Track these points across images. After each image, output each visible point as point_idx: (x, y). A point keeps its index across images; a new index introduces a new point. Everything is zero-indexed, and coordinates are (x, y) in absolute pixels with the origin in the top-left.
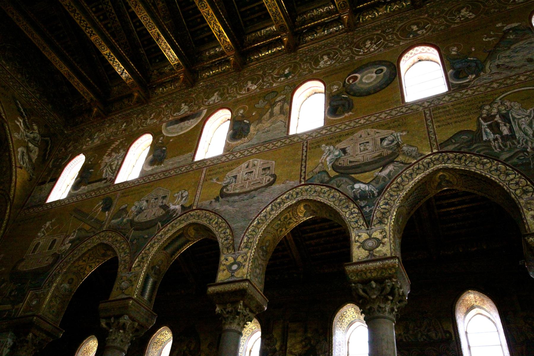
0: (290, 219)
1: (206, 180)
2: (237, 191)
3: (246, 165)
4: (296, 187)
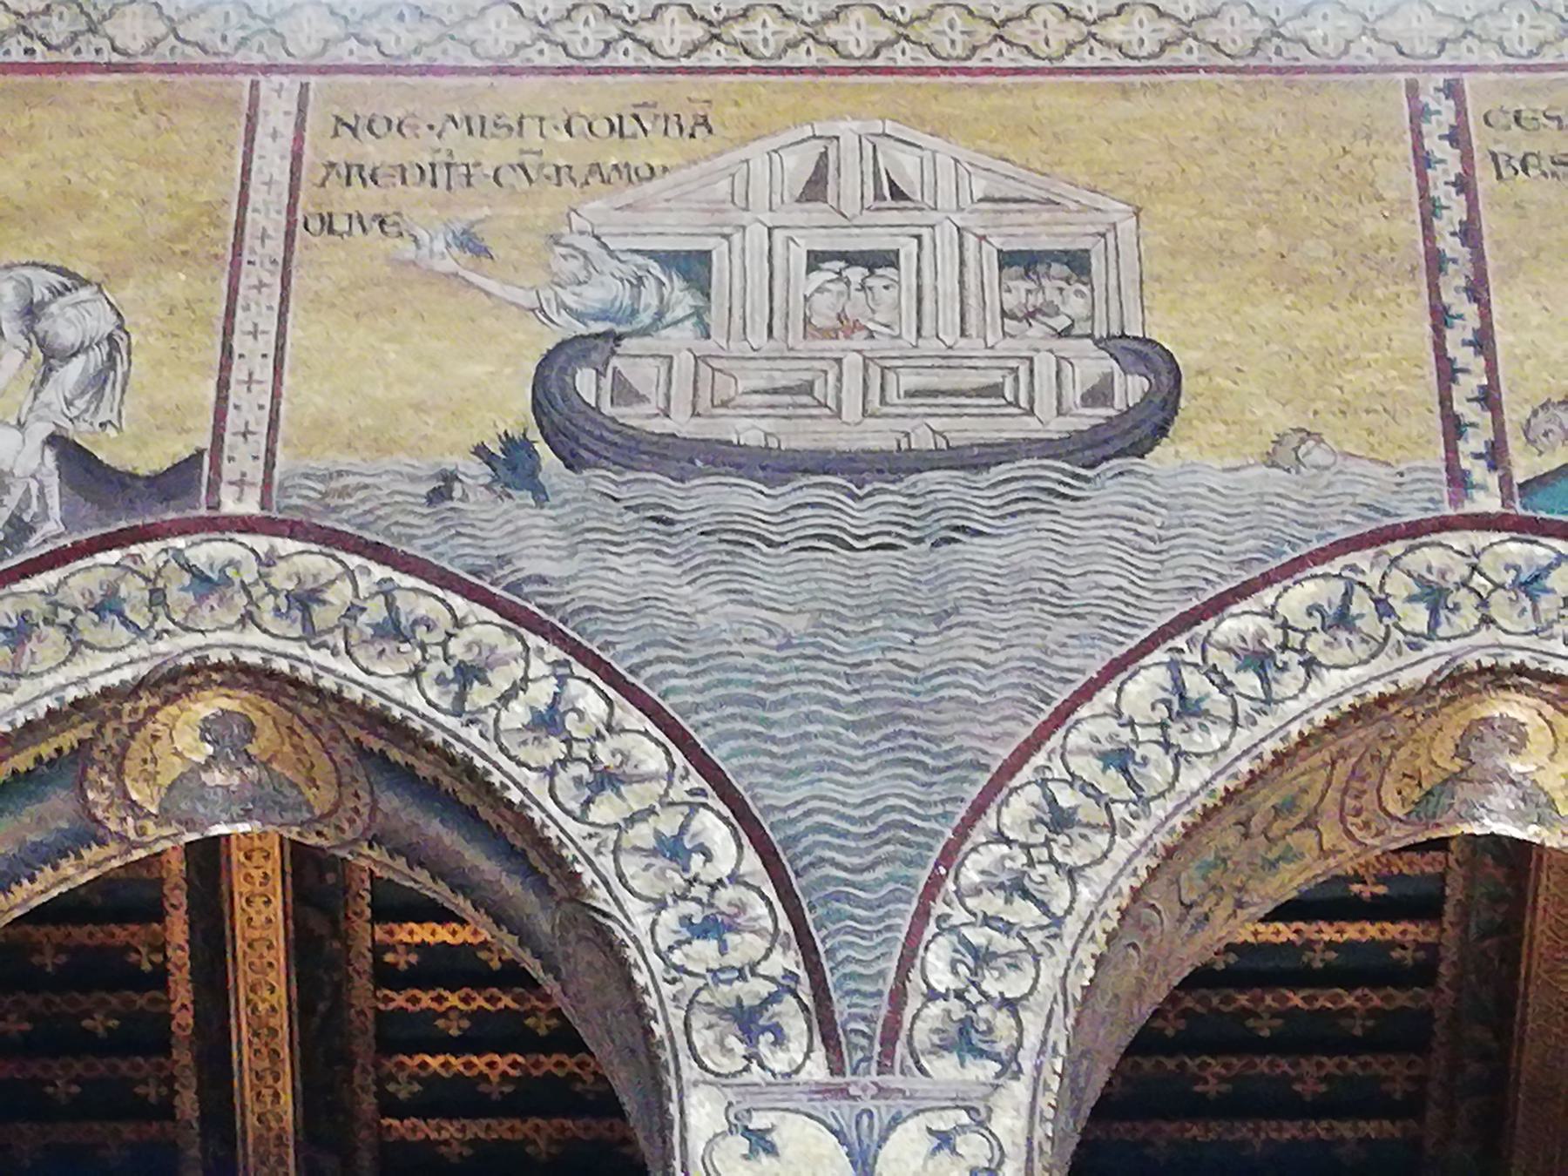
0: (1308, 824)
1: (328, 225)
2: (748, 432)
3: (798, 165)
4: (1414, 530)
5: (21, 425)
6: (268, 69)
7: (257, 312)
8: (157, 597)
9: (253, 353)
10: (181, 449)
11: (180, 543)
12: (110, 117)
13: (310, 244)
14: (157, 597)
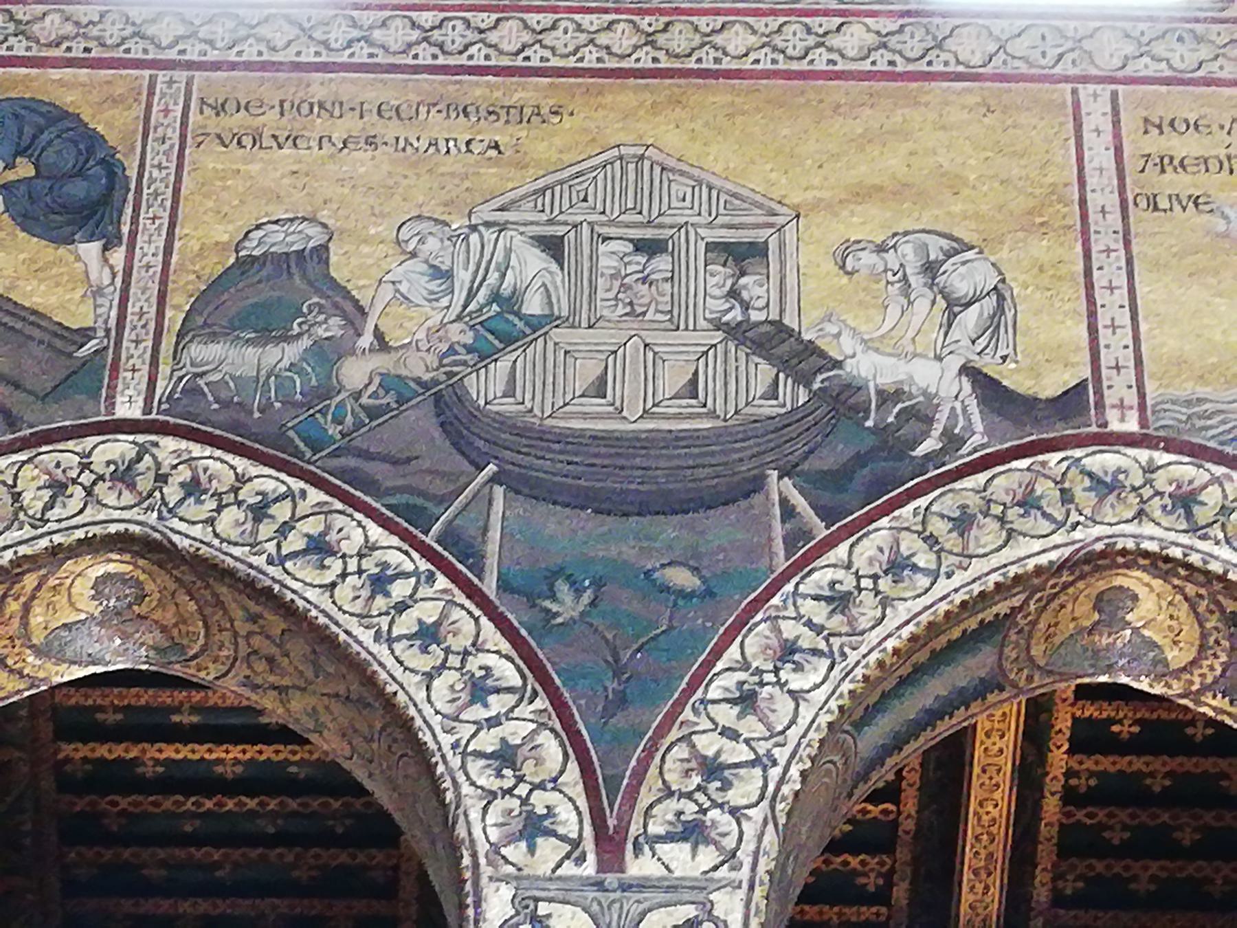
5: (939, 358)
6: (1085, 79)
7: (1110, 271)
8: (1066, 497)
9: (1112, 306)
10: (1069, 379)
11: (1078, 453)
12: (965, 116)
13: (1140, 218)
14: (1066, 497)
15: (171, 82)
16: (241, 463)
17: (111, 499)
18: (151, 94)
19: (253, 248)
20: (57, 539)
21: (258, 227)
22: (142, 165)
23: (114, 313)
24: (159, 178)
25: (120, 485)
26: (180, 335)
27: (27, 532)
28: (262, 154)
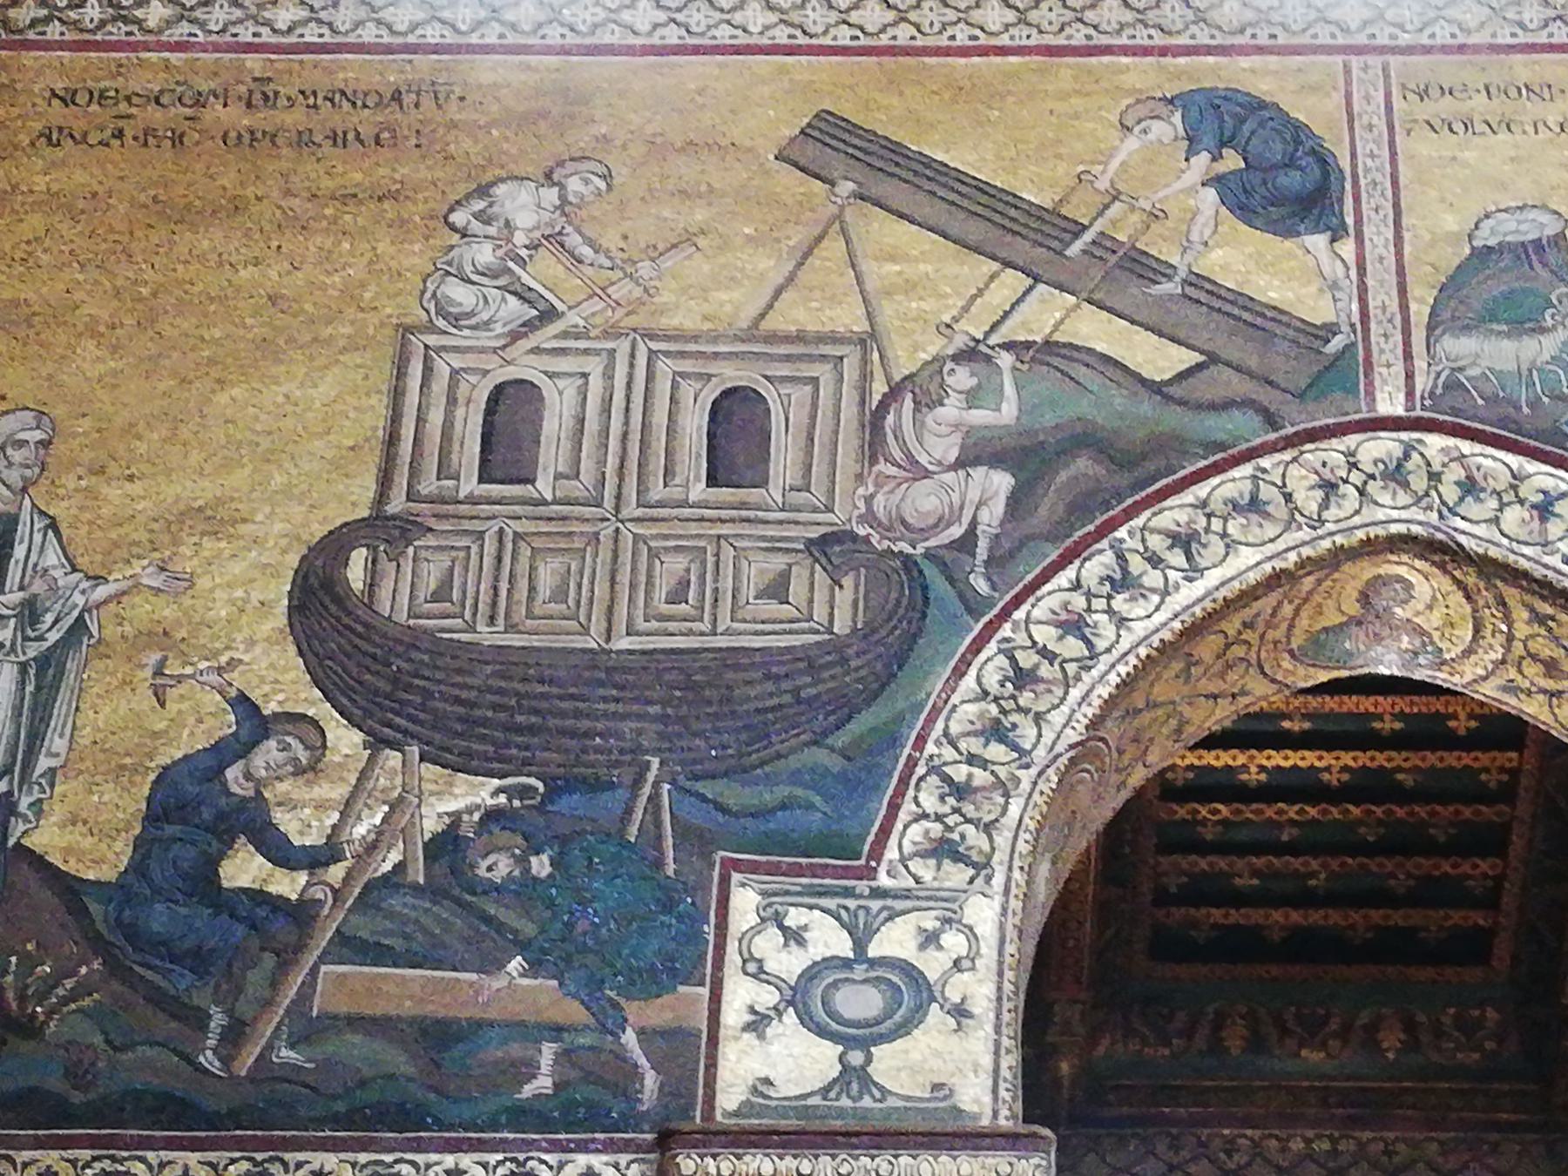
15: (1365, 68)
16: (1514, 460)
17: (1385, 498)
18: (1348, 83)
19: (1486, 238)
20: (1339, 539)
21: (1487, 216)
22: (1353, 155)
23: (1355, 307)
24: (1373, 168)
25: (1392, 485)
26: (1431, 328)
27: (1305, 534)
28: (1476, 139)
